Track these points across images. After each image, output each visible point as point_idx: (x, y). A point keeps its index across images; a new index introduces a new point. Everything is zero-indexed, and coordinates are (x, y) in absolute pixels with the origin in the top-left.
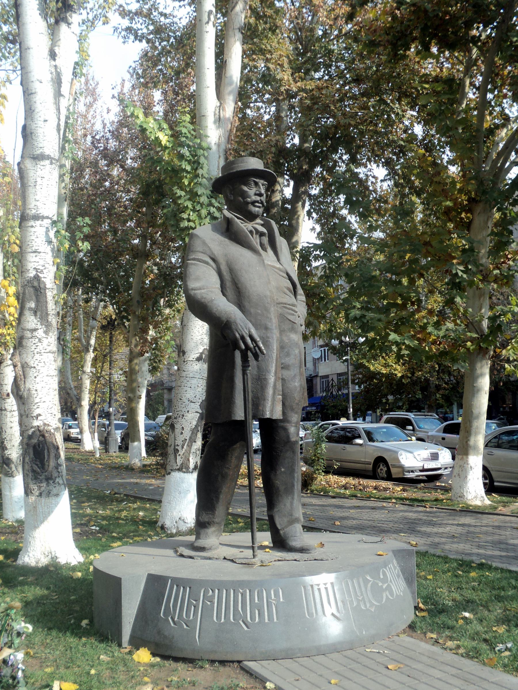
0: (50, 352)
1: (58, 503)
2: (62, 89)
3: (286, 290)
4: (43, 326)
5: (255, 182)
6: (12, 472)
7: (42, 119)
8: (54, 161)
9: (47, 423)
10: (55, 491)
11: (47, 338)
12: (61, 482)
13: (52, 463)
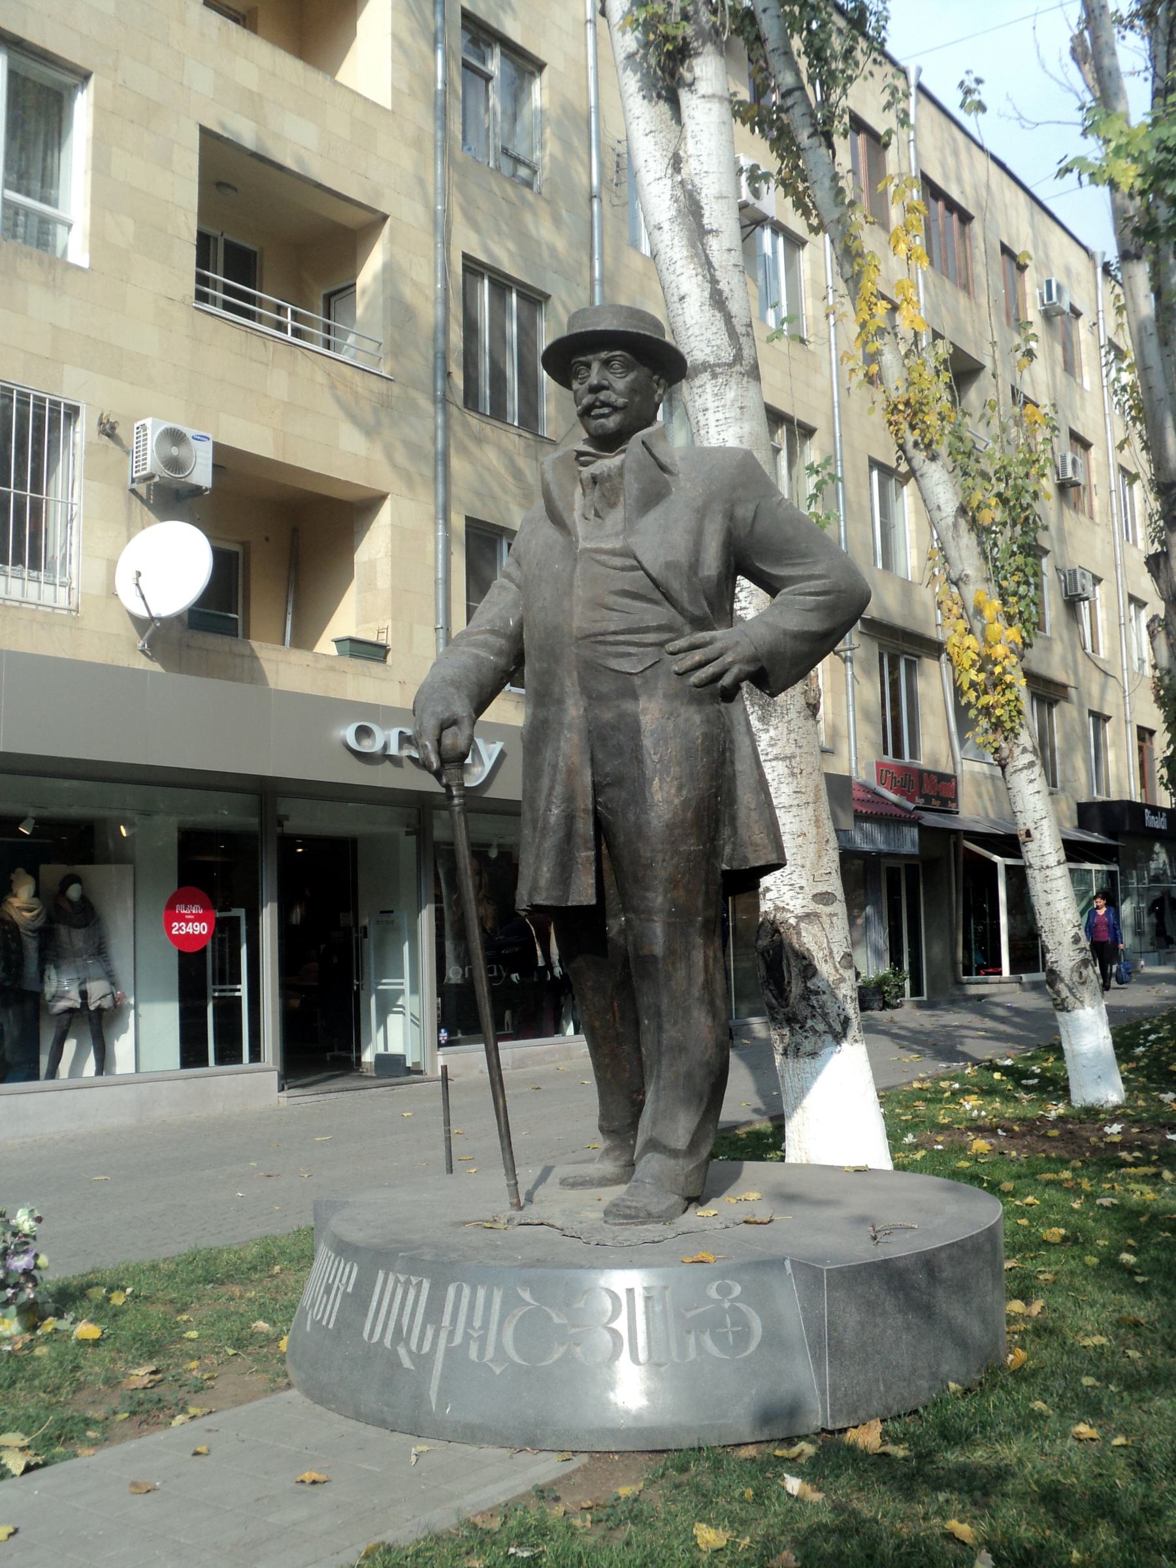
0: (776, 759)
1: (818, 1073)
2: (705, 221)
3: (612, 600)
4: (756, 708)
5: (583, 363)
6: (1063, 1000)
7: (676, 298)
8: (719, 370)
9: (781, 905)
10: (807, 1046)
11: (767, 731)
12: (821, 1027)
13: (796, 989)
